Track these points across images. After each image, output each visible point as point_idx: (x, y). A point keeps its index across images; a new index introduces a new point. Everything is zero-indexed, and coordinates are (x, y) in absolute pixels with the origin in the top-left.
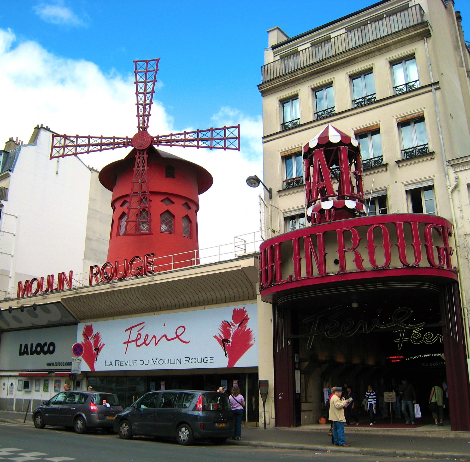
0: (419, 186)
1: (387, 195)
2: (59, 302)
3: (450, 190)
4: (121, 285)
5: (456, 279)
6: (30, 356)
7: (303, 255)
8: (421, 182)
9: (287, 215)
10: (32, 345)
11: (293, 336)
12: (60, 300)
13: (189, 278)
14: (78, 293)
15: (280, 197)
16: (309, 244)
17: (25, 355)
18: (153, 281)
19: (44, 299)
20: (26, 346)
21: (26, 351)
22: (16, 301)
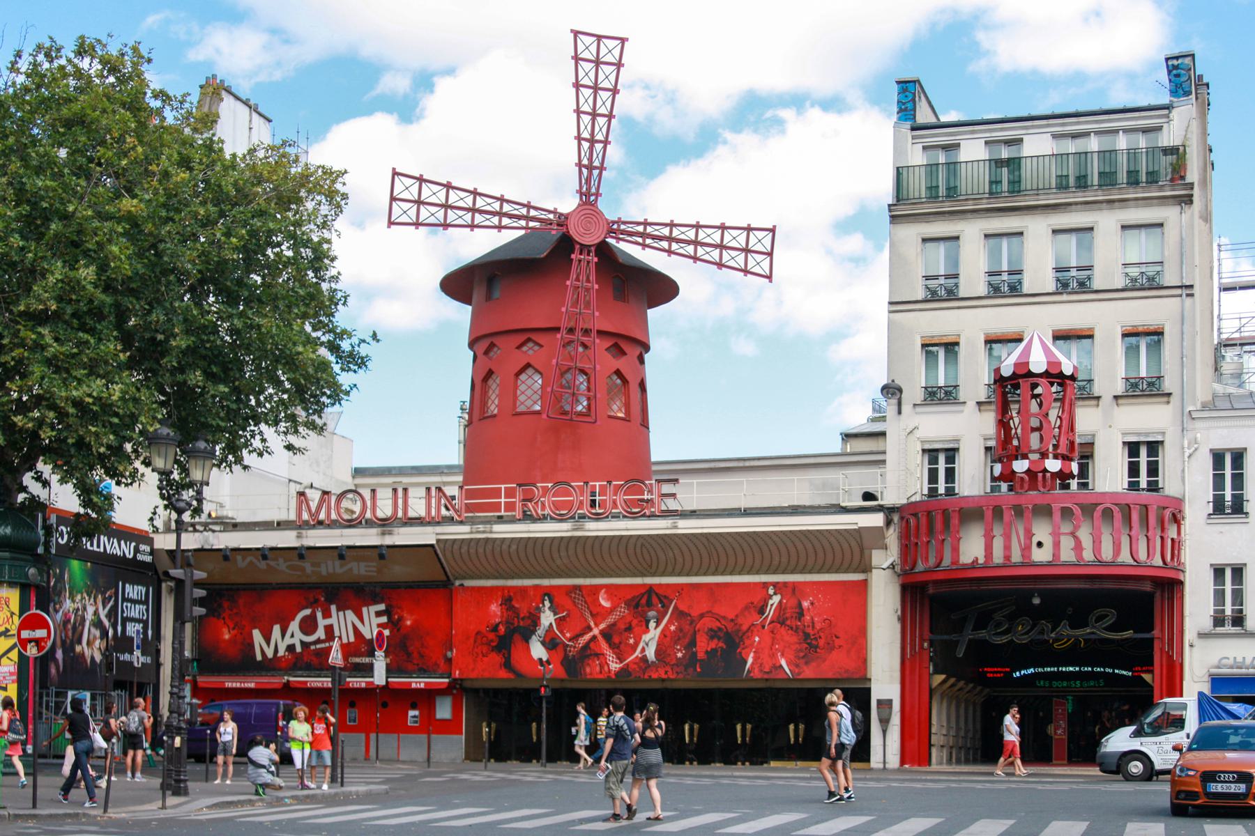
0: (1142, 439)
1: (1092, 444)
2: (432, 546)
3: (1187, 454)
4: (595, 529)
5: (1182, 579)
7: (998, 531)
8: (1147, 434)
9: (927, 446)
11: (932, 637)
12: (434, 542)
13: (754, 532)
14: (484, 532)
18: (676, 527)
19: (383, 534)
22: (293, 534)
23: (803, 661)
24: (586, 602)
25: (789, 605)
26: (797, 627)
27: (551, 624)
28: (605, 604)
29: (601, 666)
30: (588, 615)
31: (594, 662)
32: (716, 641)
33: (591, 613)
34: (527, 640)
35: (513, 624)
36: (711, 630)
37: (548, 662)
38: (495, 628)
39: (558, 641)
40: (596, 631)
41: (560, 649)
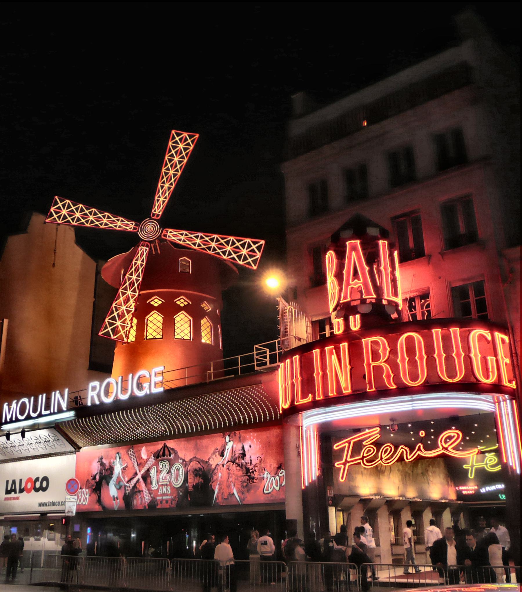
6: (17, 495)
10: (21, 480)
15: (307, 297)
16: (333, 356)
17: (13, 493)
20: (14, 482)
21: (13, 488)
23: (246, 489)
24: (135, 457)
25: (237, 449)
26: (242, 465)
27: (119, 473)
28: (144, 456)
29: (142, 500)
30: (136, 465)
31: (138, 496)
32: (198, 478)
33: (137, 463)
34: (108, 484)
35: (102, 474)
36: (196, 470)
37: (117, 498)
38: (94, 478)
39: (121, 484)
40: (139, 476)
41: (123, 489)
